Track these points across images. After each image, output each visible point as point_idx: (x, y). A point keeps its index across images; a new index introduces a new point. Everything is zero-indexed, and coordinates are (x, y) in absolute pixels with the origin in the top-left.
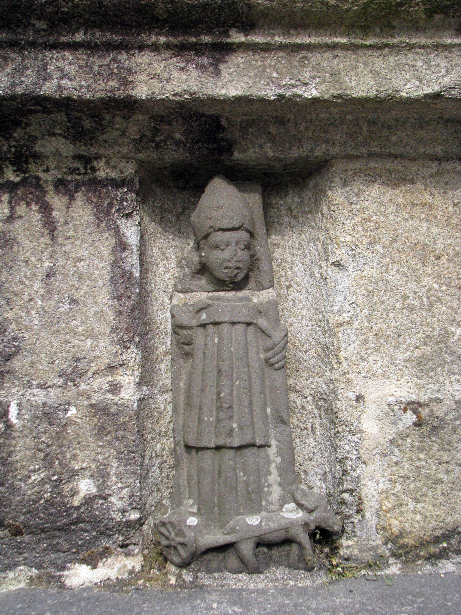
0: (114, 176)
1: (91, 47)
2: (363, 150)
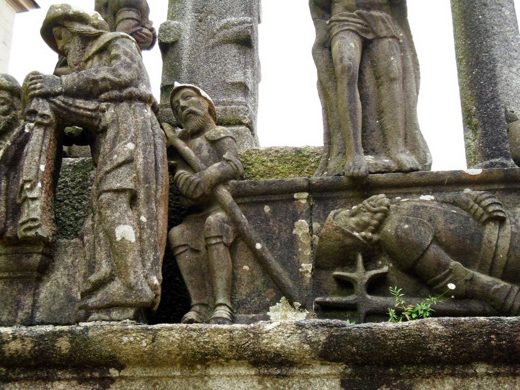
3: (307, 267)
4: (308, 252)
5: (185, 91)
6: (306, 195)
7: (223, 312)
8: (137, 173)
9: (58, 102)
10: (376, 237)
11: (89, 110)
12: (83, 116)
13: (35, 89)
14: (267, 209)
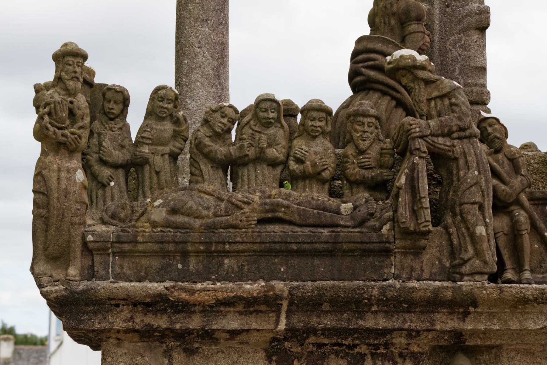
0: (420, 350)
1: (422, 312)
2: (514, 342)
5: (490, 120)
7: (527, 275)
8: (483, 192)
9: (429, 141)
11: (447, 146)
12: (443, 149)
13: (415, 132)
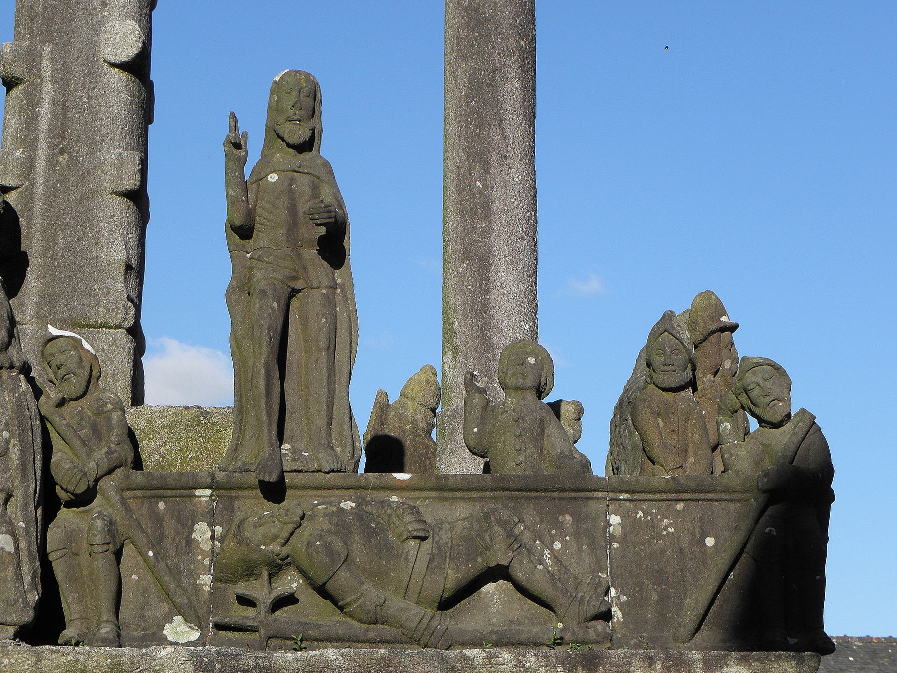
3: (206, 580)
4: (207, 561)
6: (208, 492)
10: (285, 551)
14: (162, 505)
